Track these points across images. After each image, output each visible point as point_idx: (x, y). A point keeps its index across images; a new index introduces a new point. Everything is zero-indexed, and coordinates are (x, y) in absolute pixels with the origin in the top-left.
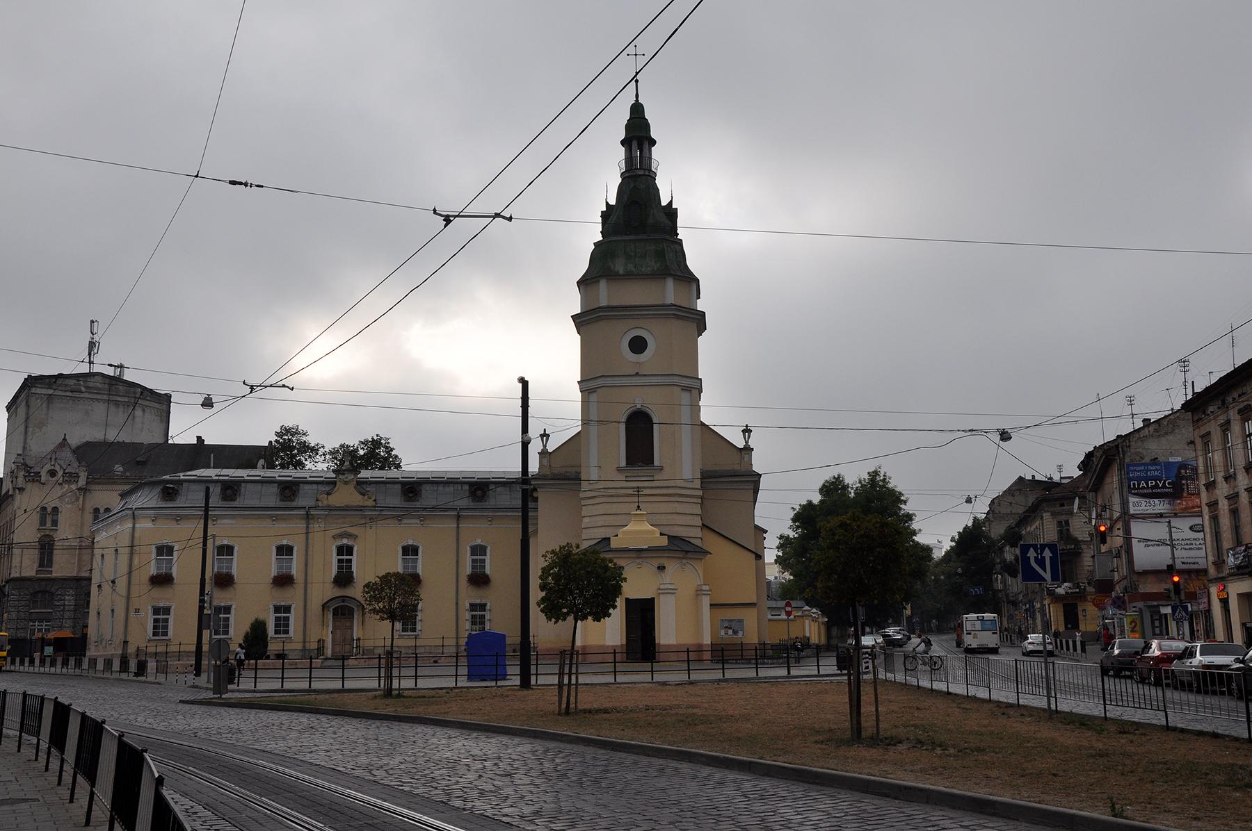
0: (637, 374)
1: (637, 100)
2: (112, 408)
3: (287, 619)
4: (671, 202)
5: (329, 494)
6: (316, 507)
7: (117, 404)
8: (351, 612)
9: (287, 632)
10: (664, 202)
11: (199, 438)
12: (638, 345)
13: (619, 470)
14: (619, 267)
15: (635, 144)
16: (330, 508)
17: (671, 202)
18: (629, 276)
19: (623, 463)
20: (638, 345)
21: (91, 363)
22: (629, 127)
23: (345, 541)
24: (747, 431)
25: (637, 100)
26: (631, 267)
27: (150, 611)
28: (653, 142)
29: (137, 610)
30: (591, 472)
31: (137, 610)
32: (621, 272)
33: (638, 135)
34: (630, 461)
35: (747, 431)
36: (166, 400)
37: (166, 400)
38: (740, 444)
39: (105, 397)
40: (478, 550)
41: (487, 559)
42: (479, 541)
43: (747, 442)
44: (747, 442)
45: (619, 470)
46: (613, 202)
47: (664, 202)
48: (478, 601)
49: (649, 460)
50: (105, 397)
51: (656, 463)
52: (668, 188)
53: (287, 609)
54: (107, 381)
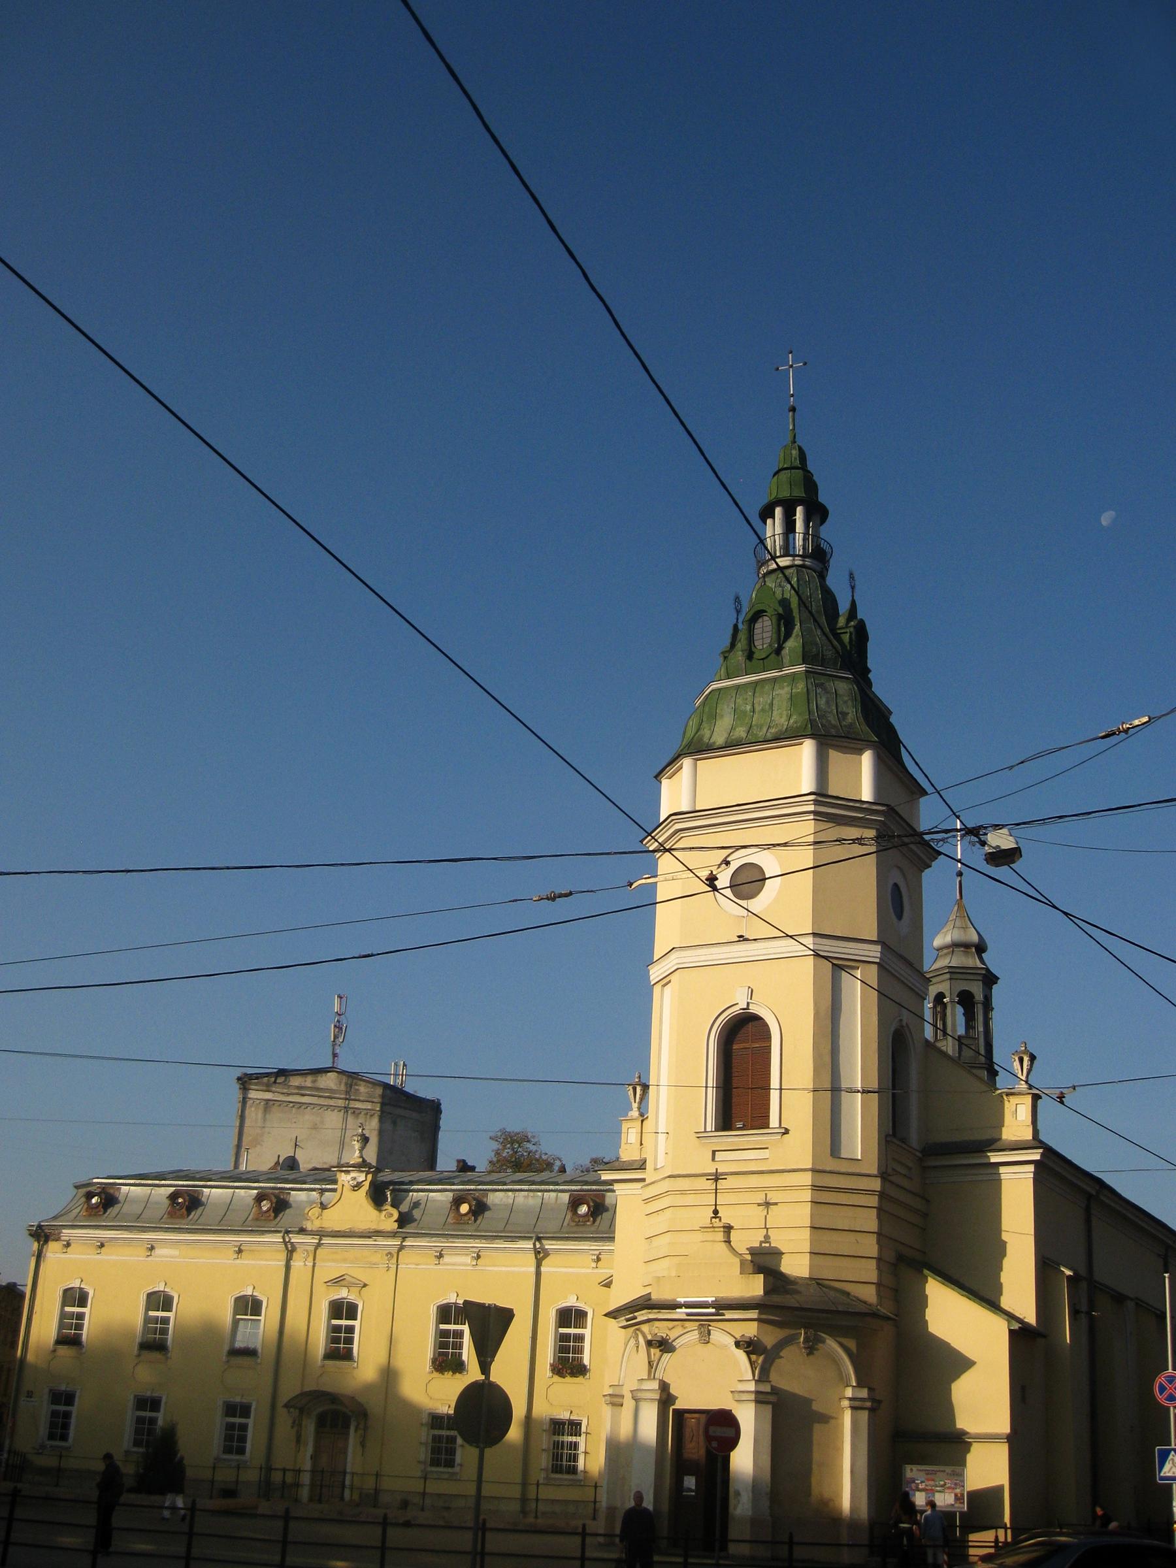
0: (742, 938)
2: (350, 1119)
3: (244, 1427)
5: (323, 1207)
6: (302, 1231)
7: (356, 1112)
8: (347, 1426)
9: (241, 1451)
11: (459, 1161)
16: (322, 1234)
18: (732, 746)
19: (710, 1126)
21: (335, 1055)
23: (343, 1293)
26: (741, 732)
27: (46, 1397)
29: (30, 1394)
31: (30, 1394)
34: (726, 1120)
36: (433, 1109)
37: (433, 1109)
39: (341, 1103)
42: (571, 1301)
45: (701, 1136)
49: (760, 1120)
50: (341, 1103)
51: (774, 1121)
53: (245, 1410)
54: (344, 1079)
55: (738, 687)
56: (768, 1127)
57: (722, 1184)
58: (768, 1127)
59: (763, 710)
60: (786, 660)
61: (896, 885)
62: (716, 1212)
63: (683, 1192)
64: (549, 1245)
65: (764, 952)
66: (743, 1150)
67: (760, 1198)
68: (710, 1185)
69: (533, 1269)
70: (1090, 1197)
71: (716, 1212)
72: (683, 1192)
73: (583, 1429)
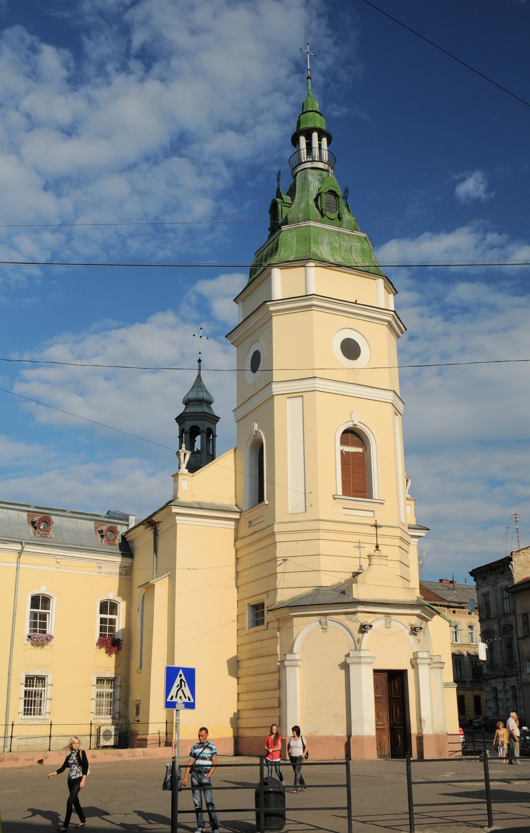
12: (350, 349)
14: (325, 252)
15: (315, 135)
19: (340, 492)
20: (350, 349)
32: (332, 260)
42: (42, 590)
48: (37, 672)
55: (327, 230)
56: (372, 498)
57: (380, 531)
58: (372, 498)
59: (346, 250)
60: (345, 225)
62: (377, 547)
64: (27, 548)
65: (367, 394)
66: (358, 510)
68: (373, 530)
69: (15, 565)
71: (377, 547)
73: (49, 681)
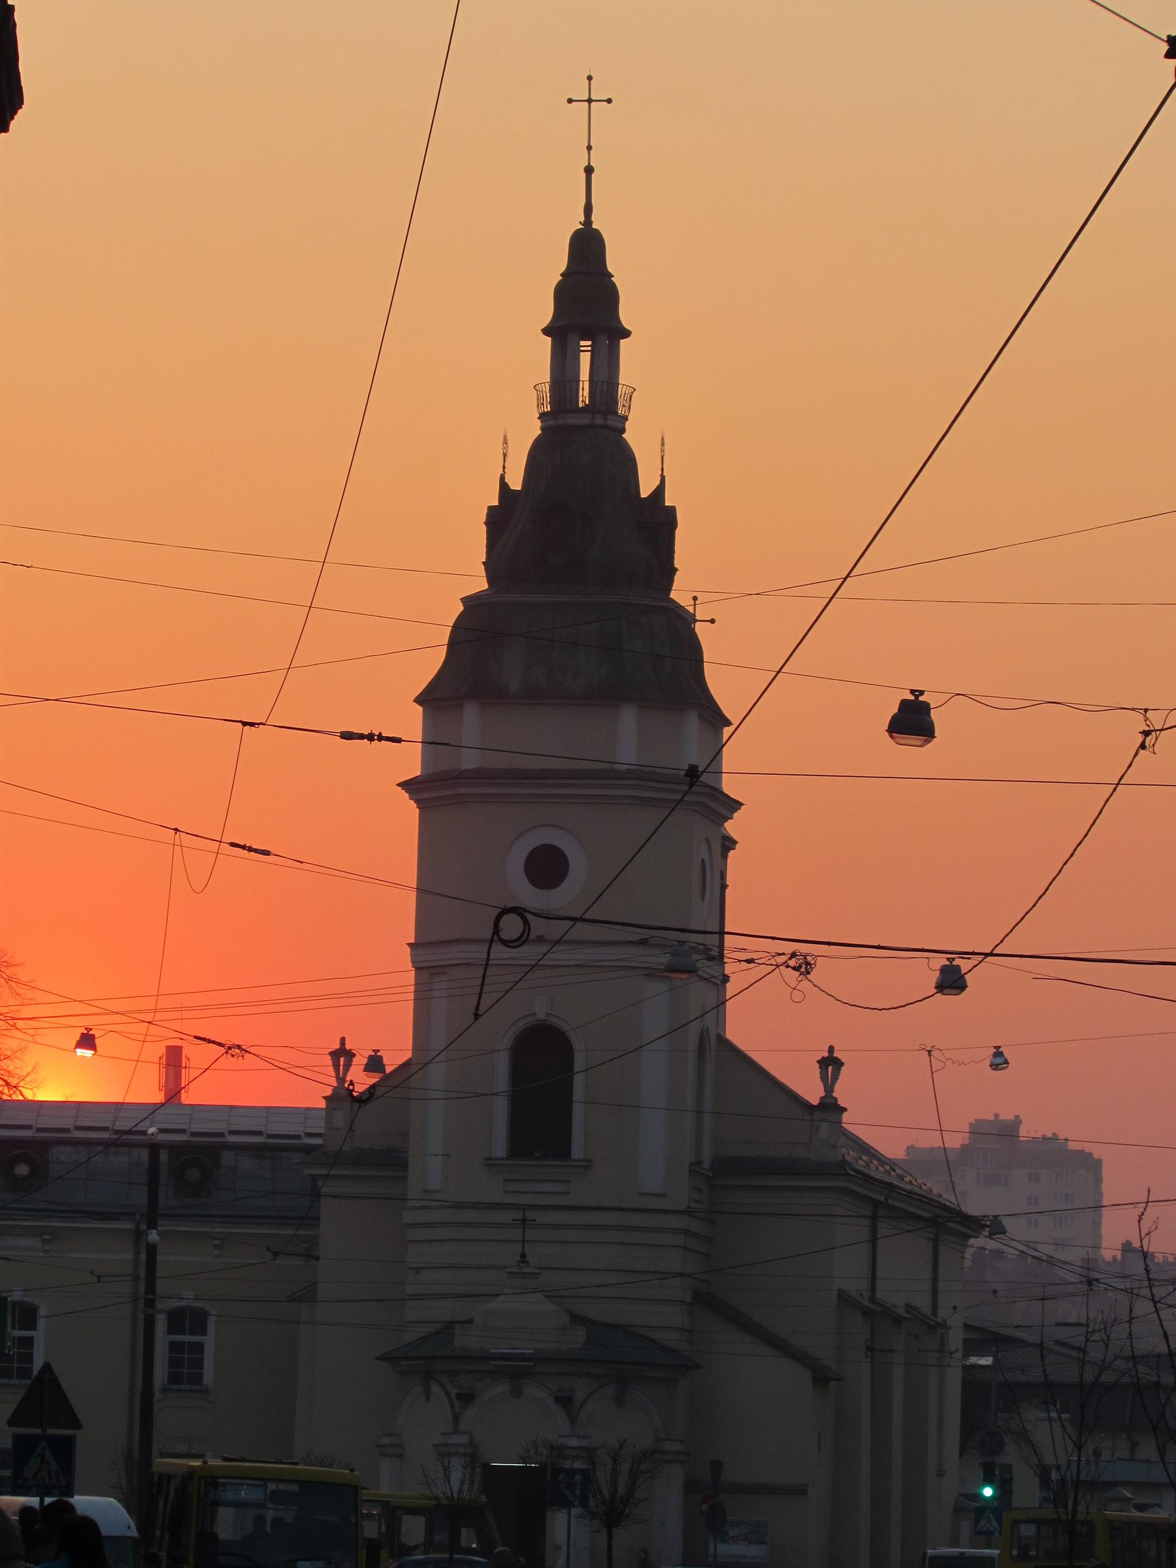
1: (588, 222)
4: (660, 491)
10: (645, 492)
13: (490, 1163)
17: (660, 491)
19: (500, 1149)
20: (547, 867)
22: (563, 294)
24: (830, 1064)
25: (588, 222)
28: (626, 334)
30: (430, 1170)
33: (586, 305)
35: (830, 1064)
38: (813, 1092)
40: (189, 1320)
41: (209, 1341)
43: (829, 1089)
44: (829, 1089)
46: (516, 484)
47: (645, 492)
52: (662, 439)
61: (703, 860)
62: (523, 1256)
63: (469, 1225)
67: (518, 1215)
70: (876, 1204)
71: (523, 1256)
72: (469, 1225)
